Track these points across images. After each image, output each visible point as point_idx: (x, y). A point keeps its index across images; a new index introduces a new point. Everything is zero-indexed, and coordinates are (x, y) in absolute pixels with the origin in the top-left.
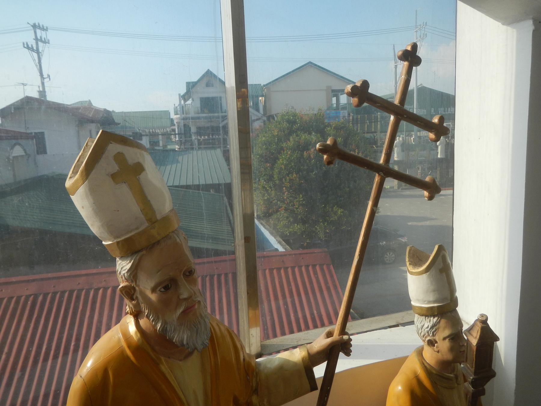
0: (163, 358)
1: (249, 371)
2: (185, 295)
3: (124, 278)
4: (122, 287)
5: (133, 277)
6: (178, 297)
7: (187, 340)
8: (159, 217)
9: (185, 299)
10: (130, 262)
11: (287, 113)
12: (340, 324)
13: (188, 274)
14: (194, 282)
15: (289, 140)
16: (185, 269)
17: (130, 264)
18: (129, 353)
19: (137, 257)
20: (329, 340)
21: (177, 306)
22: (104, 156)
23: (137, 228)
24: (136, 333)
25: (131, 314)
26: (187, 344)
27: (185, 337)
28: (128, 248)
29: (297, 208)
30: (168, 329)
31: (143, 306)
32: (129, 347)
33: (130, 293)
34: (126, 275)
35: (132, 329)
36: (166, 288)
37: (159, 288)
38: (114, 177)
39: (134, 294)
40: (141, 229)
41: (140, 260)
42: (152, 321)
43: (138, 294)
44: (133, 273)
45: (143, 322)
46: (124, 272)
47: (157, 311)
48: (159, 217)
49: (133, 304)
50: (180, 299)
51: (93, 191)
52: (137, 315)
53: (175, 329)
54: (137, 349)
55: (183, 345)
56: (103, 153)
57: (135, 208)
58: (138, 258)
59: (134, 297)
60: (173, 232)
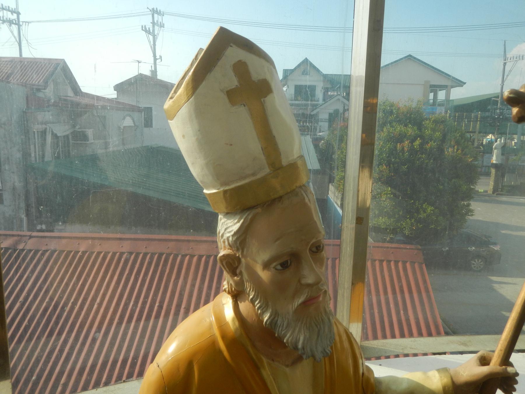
0: (265, 360)
2: (310, 280)
3: (227, 243)
4: (224, 255)
5: (240, 243)
6: (299, 281)
7: (303, 343)
8: (284, 162)
9: (309, 285)
10: (238, 222)
11: (384, 103)
12: (503, 349)
13: (314, 249)
14: (320, 262)
15: (382, 131)
16: (314, 241)
17: (238, 225)
18: (222, 345)
19: (249, 215)
20: (485, 370)
21: (296, 294)
22: (219, 63)
23: (253, 174)
24: (233, 320)
25: (229, 293)
26: (303, 348)
27: (302, 338)
28: (239, 201)
29: (384, 201)
30: (279, 322)
31: (248, 286)
32: (223, 337)
33: (232, 264)
34: (230, 239)
35: (229, 313)
36: (285, 265)
37: (274, 264)
38: (232, 95)
39: (237, 268)
40: (259, 176)
41: (252, 220)
42: (258, 309)
43: (242, 268)
44: (242, 238)
45: (243, 306)
46: (228, 235)
47: (267, 296)
48: (285, 162)
49: (235, 282)
50: (301, 284)
51: (201, 113)
53: (288, 325)
54: (233, 343)
55: (296, 348)
56: (218, 60)
57: (254, 145)
58: (250, 217)
59: (238, 272)
60: (300, 187)
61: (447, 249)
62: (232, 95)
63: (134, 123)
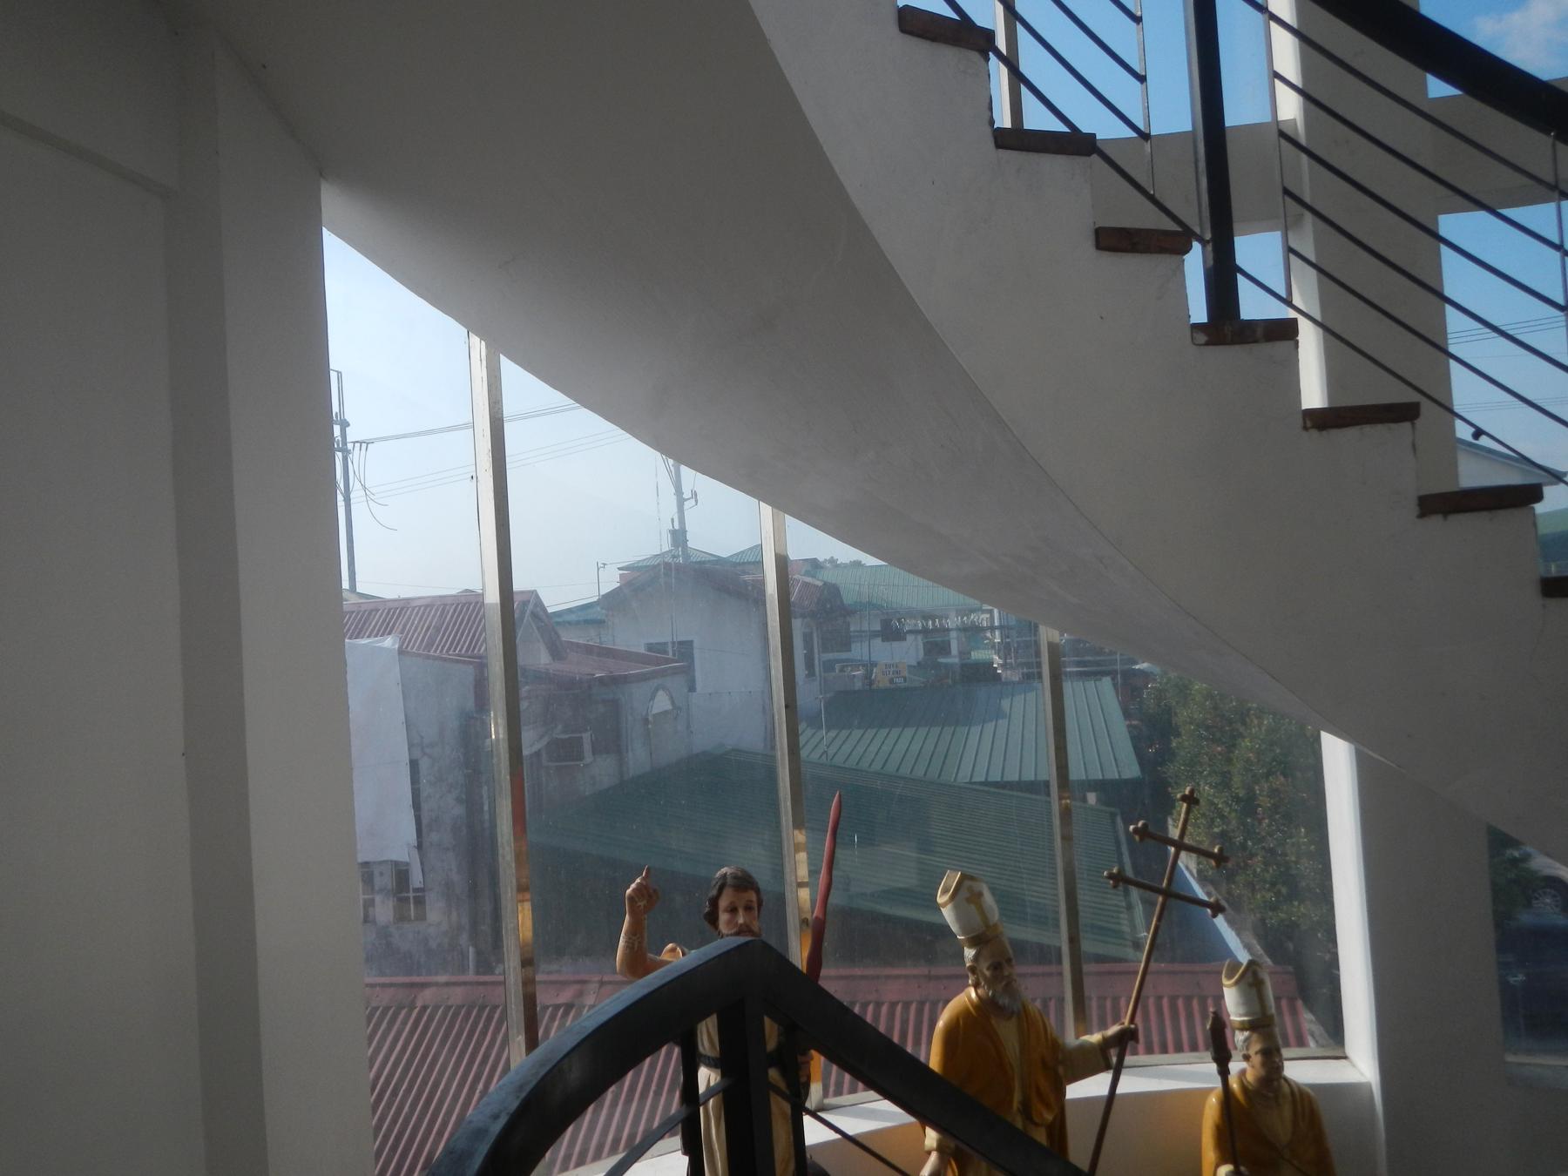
1: (1056, 1046)
28: (975, 941)
33: (973, 970)
35: (973, 995)
44: (976, 958)
47: (991, 983)
51: (957, 908)
52: (976, 986)
54: (976, 1007)
61: (1521, 977)
62: (968, 900)
63: (673, 703)
